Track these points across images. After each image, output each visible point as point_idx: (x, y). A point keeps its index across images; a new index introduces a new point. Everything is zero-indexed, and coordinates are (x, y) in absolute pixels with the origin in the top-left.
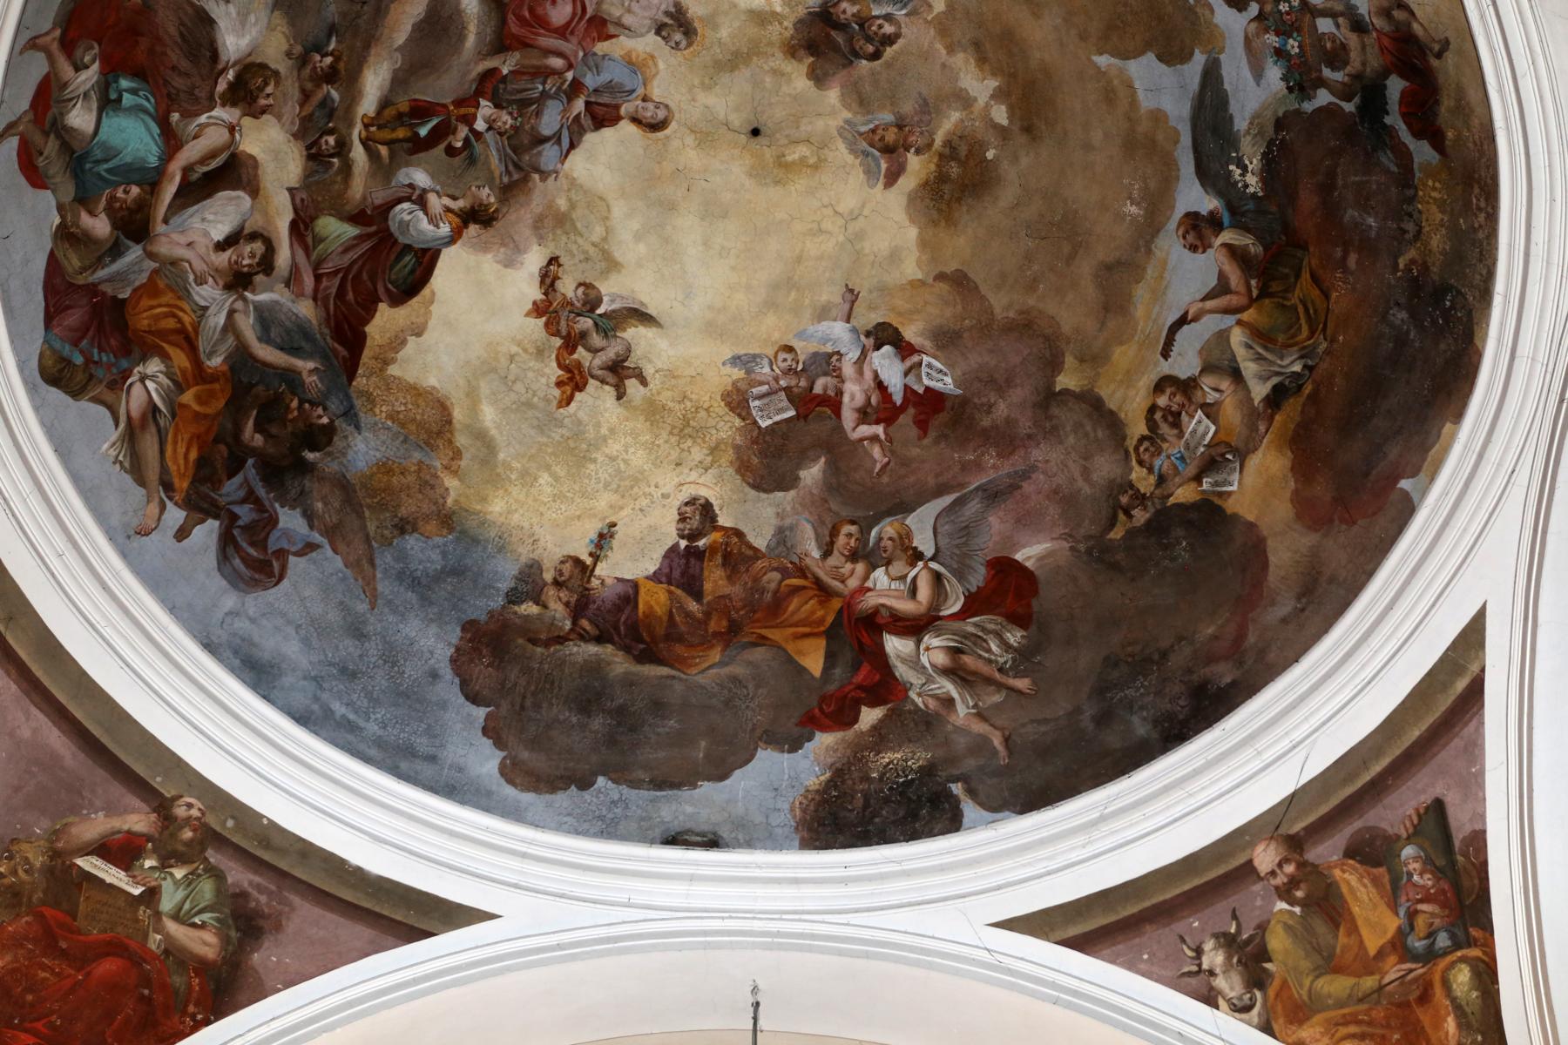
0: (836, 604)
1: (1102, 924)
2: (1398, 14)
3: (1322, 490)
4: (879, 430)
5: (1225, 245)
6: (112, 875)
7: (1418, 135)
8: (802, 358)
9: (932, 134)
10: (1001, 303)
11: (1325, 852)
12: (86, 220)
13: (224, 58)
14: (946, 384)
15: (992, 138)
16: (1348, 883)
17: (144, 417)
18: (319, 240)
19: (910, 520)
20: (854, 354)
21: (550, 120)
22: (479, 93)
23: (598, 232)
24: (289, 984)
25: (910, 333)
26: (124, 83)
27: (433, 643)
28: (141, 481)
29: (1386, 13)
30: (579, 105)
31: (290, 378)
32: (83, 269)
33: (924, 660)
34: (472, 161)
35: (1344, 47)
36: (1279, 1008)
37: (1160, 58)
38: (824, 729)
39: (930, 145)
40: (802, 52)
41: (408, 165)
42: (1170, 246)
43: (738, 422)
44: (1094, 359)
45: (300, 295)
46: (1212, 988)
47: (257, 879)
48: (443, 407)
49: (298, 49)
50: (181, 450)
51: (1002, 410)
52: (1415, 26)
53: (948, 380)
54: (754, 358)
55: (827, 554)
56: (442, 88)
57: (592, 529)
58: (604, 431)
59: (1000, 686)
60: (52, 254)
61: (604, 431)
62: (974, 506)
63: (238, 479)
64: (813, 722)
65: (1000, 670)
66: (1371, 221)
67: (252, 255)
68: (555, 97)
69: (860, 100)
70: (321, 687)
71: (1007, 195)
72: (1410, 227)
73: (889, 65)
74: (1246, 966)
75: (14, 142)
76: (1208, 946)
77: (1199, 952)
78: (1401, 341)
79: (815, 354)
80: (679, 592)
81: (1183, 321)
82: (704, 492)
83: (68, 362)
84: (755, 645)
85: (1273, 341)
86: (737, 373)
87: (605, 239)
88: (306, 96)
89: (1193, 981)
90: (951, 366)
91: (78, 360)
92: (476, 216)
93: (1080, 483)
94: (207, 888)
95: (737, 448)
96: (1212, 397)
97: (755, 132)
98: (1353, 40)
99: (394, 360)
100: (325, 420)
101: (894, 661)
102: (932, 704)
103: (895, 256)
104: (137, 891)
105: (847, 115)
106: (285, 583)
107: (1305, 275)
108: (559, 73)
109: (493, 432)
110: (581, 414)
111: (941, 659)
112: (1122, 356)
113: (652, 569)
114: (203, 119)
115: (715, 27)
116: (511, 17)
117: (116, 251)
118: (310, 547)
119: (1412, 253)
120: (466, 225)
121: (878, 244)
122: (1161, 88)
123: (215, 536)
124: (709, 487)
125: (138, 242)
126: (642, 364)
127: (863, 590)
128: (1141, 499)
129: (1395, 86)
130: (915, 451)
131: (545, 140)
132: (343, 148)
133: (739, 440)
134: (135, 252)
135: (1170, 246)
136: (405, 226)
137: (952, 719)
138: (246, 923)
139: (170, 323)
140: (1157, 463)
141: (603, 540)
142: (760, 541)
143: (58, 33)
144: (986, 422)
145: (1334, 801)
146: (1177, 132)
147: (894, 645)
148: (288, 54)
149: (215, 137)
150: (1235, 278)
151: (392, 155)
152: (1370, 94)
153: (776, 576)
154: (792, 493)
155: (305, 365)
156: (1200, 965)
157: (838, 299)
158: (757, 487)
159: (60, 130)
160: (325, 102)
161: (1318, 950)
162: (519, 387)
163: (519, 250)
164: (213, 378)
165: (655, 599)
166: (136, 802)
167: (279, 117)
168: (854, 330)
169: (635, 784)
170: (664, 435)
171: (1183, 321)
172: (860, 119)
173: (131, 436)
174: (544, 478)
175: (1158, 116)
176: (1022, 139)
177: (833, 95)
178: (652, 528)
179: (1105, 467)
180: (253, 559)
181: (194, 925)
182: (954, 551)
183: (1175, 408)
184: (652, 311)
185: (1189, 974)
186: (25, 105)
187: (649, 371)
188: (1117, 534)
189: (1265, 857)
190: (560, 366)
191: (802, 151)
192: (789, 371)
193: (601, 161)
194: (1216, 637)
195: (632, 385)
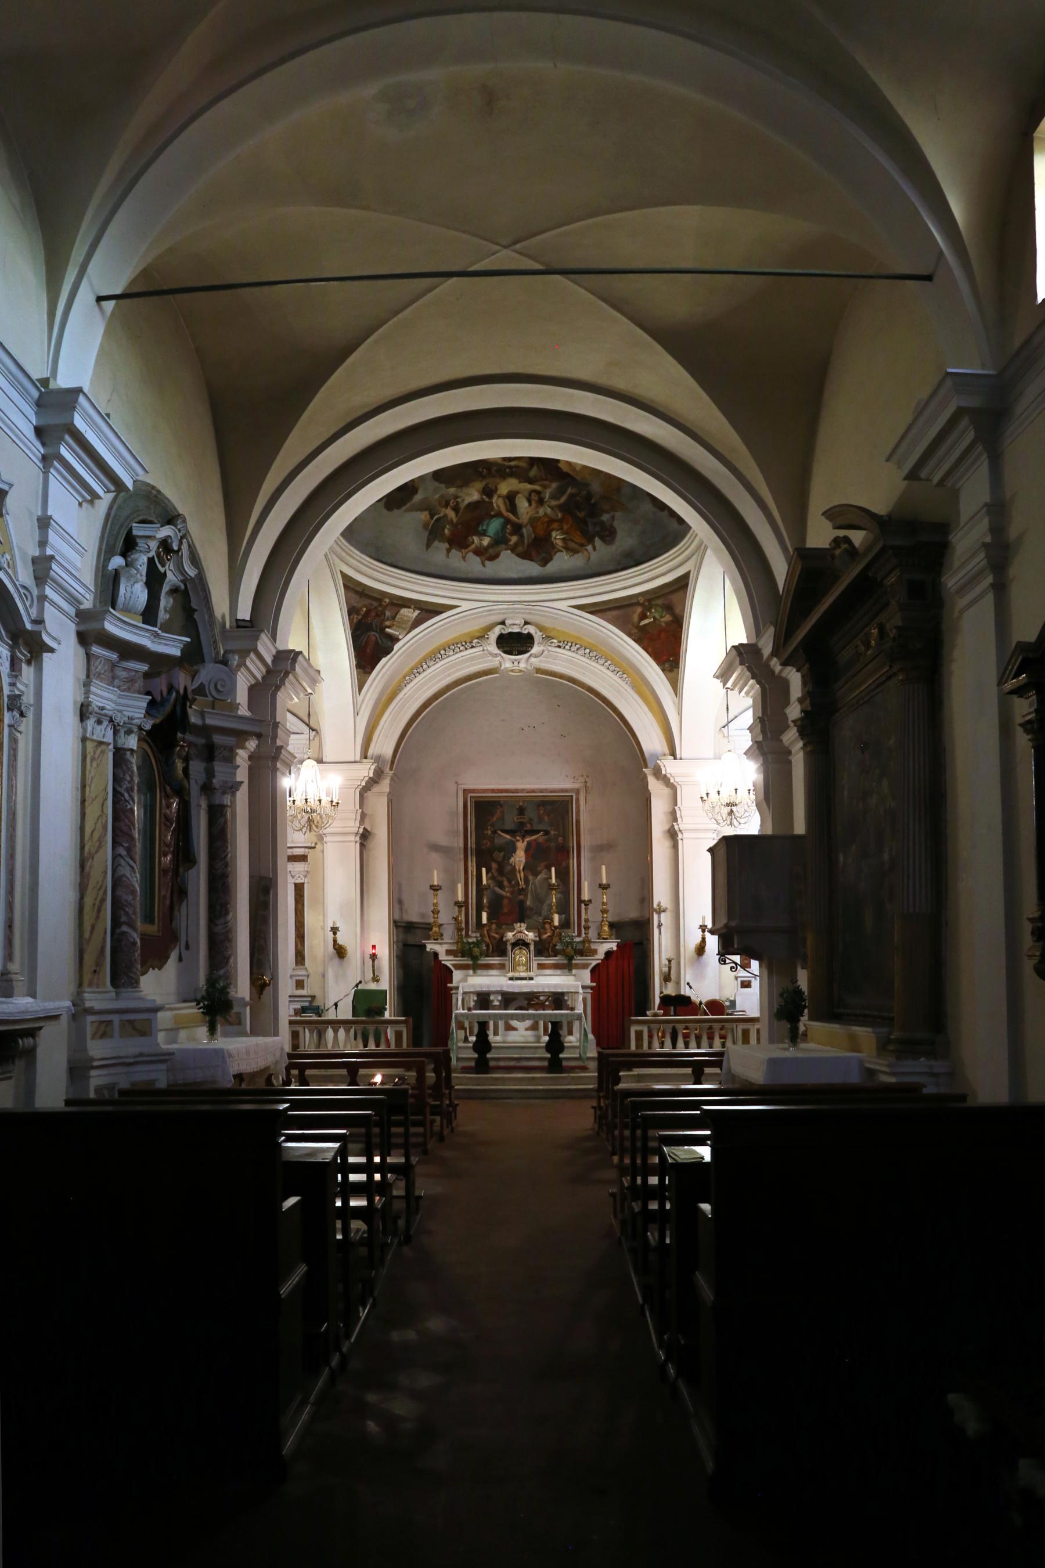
12: (512, 543)
28: (578, 552)
31: (571, 496)
88: (494, 476)
117: (522, 536)
132: (510, 467)
134: (524, 531)
149: (501, 502)
155: (569, 490)
159: (486, 549)
173: (567, 549)
186: (478, 559)
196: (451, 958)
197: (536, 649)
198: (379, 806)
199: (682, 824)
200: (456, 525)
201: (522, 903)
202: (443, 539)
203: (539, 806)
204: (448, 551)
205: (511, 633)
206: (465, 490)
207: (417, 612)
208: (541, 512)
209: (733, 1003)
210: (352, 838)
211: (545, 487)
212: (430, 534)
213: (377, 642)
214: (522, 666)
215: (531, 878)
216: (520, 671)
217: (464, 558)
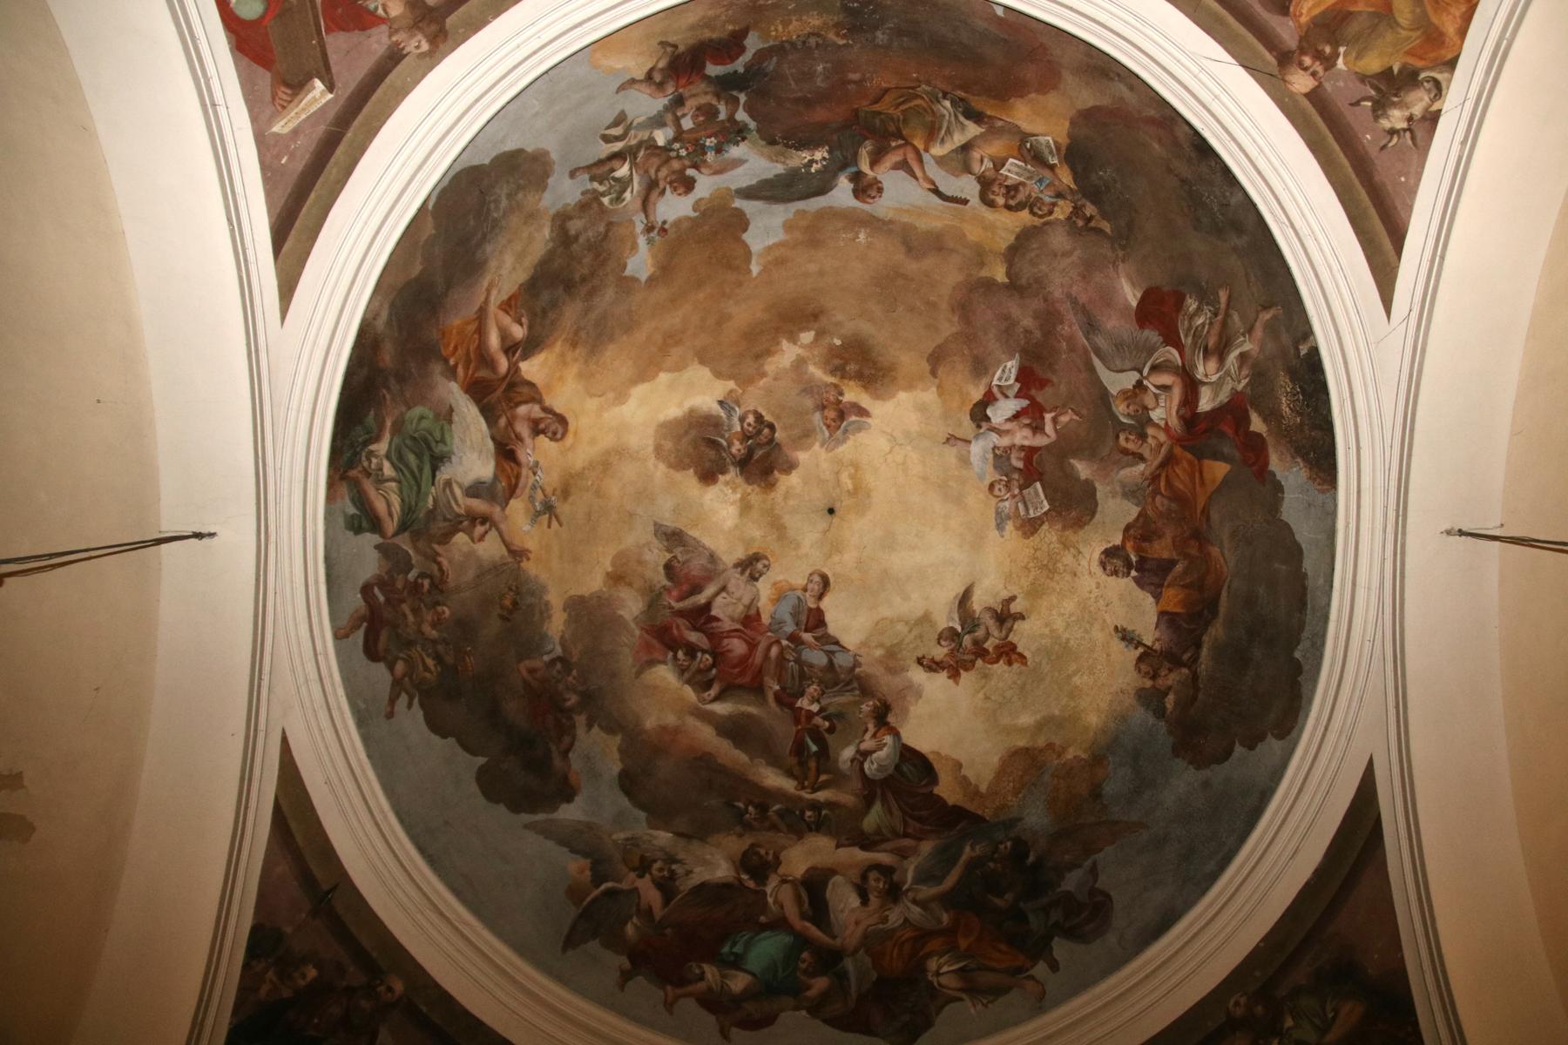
0: (1178, 450)
1: (1379, 221)
2: (657, 77)
3: (1030, 72)
4: (1048, 417)
5: (872, 167)
7: (742, 50)
8: (998, 477)
9: (827, 385)
10: (948, 327)
11: (1287, 31)
12: (812, 993)
13: (731, 880)
14: (1012, 365)
15: (827, 340)
16: (1310, 9)
18: (878, 831)
19: (1114, 391)
20: (994, 437)
21: (817, 658)
22: (791, 706)
24: (1399, 948)
25: (977, 394)
26: (726, 949)
27: (1183, 781)
29: (660, 86)
30: (807, 637)
31: (973, 864)
33: (1214, 378)
34: (840, 716)
35: (698, 109)
36: (1432, 55)
37: (745, 230)
38: (1267, 463)
39: (836, 386)
40: (771, 479)
41: (836, 761)
42: (883, 206)
43: (1045, 527)
44: (980, 255)
45: (915, 851)
46: (1423, 118)
48: (1016, 753)
49: (738, 829)
51: (1027, 322)
52: (661, 65)
53: (1009, 364)
54: (998, 513)
55: (1142, 458)
56: (784, 731)
57: (1118, 646)
58: (1047, 631)
59: (1227, 315)
60: (825, 1021)
61: (1047, 631)
62: (1100, 341)
63: (1031, 918)
64: (1262, 473)
65: (1216, 315)
66: (820, 68)
67: (877, 880)
68: (799, 653)
69: (807, 435)
71: (866, 328)
72: (812, 41)
73: (778, 418)
74: (1399, 89)
75: (734, 1030)
76: (1386, 124)
77: (1392, 132)
78: (899, 32)
79: (995, 467)
80: (1169, 578)
81: (936, 191)
82: (1097, 555)
84: (1208, 519)
85: (933, 123)
86: (1009, 526)
88: (774, 827)
89: (1419, 134)
90: (999, 363)
92: (882, 716)
93: (1074, 257)
95: (1064, 528)
96: (988, 164)
97: (831, 511)
98: (691, 104)
99: (977, 787)
100: (1009, 844)
101: (1216, 403)
102: (1245, 372)
103: (922, 408)
105: (817, 446)
107: (877, 107)
110: (1033, 648)
111: (1212, 365)
112: (973, 234)
113: (1151, 599)
114: (770, 900)
115: (753, 539)
116: (739, 681)
117: (842, 976)
118: (1093, 870)
119: (831, 36)
120: (886, 724)
121: (912, 421)
122: (767, 227)
125: (841, 959)
126: (999, 600)
127: (1167, 429)
128: (1077, 210)
129: (713, 70)
130: (1063, 388)
131: (831, 662)
132: (816, 806)
133: (1059, 526)
134: (849, 964)
135: (883, 206)
136: (881, 768)
137: (1254, 354)
140: (1048, 200)
141: (1126, 637)
142: (1134, 511)
143: (669, 988)
144: (1038, 334)
145: (1242, 30)
146: (798, 212)
147: (1205, 403)
148: (740, 836)
149: (786, 894)
150: (895, 157)
151: (826, 772)
152: (726, 86)
153: (1158, 498)
154: (1097, 485)
156: (1405, 130)
157: (954, 450)
158: (1093, 514)
159: (738, 1000)
160: (780, 814)
161: (1374, 28)
162: (1009, 694)
163: (910, 686)
165: (1173, 598)
167: (784, 848)
168: (977, 437)
169: (1301, 628)
170: (1053, 584)
171: (936, 191)
172: (819, 437)
173: (972, 989)
174: (1076, 680)
175: (788, 226)
176: (824, 321)
177: (802, 456)
178: (1121, 597)
179: (1059, 239)
180: (1088, 916)
181: (1334, 1018)
182: (1133, 354)
183: (1003, 190)
184: (961, 590)
185: (1413, 138)
186: (712, 1019)
187: (1005, 594)
188: (1106, 227)
189: (1301, 83)
190: (997, 661)
192: (1008, 486)
193: (848, 622)
194: (1160, 141)
195: (1015, 608)
202: (615, 941)
204: (626, 977)
206: (695, 845)
208: (895, 917)
211: (903, 854)
212: (581, 916)
217: (669, 1006)
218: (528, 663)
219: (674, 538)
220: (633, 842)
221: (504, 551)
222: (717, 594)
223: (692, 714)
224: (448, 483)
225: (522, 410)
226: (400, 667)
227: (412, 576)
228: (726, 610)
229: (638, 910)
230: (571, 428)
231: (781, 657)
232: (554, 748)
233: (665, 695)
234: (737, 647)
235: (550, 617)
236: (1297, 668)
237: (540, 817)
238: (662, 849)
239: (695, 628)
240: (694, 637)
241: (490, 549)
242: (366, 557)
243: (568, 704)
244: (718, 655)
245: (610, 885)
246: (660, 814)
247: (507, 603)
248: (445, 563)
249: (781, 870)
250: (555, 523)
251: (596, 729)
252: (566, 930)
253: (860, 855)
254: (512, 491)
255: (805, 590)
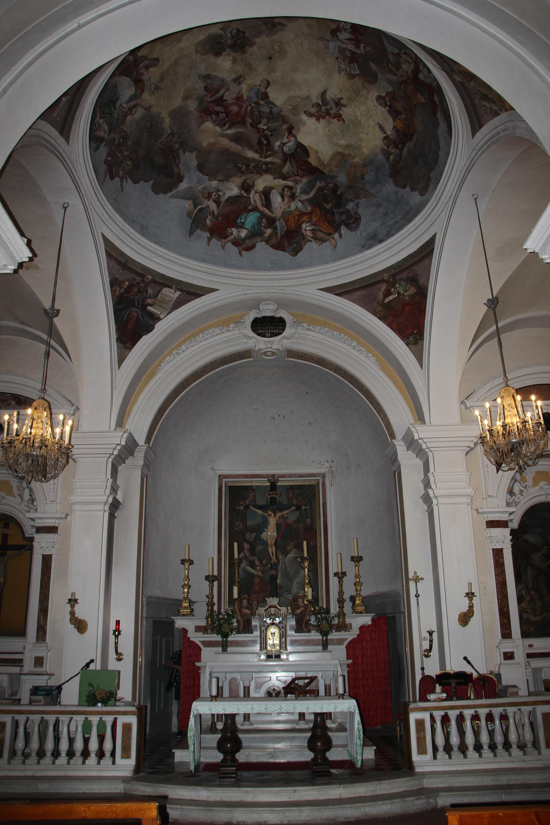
4: (362, 45)
6: (391, 298)
8: (340, 56)
13: (238, 194)
17: (314, 234)
18: (288, 173)
20: (339, 43)
21: (265, 109)
22: (256, 128)
23: (298, 99)
26: (239, 221)
27: (389, 187)
30: (262, 102)
31: (320, 189)
32: (277, 239)
34: (275, 130)
43: (357, 78)
45: (300, 181)
47: (406, 273)
48: (338, 153)
49: (240, 174)
50: (324, 226)
54: (339, 68)
56: (254, 137)
57: (377, 130)
58: (353, 114)
60: (271, 246)
61: (353, 114)
63: (336, 215)
64: (435, 113)
67: (288, 192)
70: (385, 223)
75: (243, 252)
77: (485, 106)
83: (295, 248)
86: (343, 73)
87: (301, 98)
88: (252, 172)
91: (295, 245)
92: (290, 130)
94: (403, 283)
97: (270, 58)
99: (323, 161)
100: (332, 184)
104: (397, 295)
106: (362, 216)
108: (252, 107)
109: (347, 143)
113: (392, 120)
114: (252, 200)
117: (275, 229)
118: (357, 205)
120: (292, 133)
123: (345, 228)
124: (374, 94)
127: (407, 72)
131: (271, 111)
132: (266, 164)
134: (278, 223)
136: (290, 149)
138: (413, 280)
139: (296, 218)
142: (390, 89)
143: (223, 240)
148: (240, 177)
151: (270, 151)
155: (318, 185)
160: (254, 167)
162: (337, 131)
163: (301, 121)
164: (312, 211)
166: (380, 285)
167: (256, 180)
168: (332, 41)
173: (315, 238)
177: (258, 40)
180: (353, 221)
184: (323, 90)
186: (235, 249)
187: (339, 96)
190: (334, 118)
191: (276, 47)
192: (344, 60)
193: (278, 97)
195: (342, 102)
196: (200, 634)
197: (288, 331)
198: (132, 474)
199: (436, 490)
200: (216, 217)
201: (274, 578)
202: (204, 228)
203: (288, 489)
204: (209, 240)
205: (264, 318)
206: (226, 183)
207: (178, 293)
208: (293, 206)
209: (499, 676)
210: (101, 507)
211: (296, 182)
212: (193, 222)
213: (138, 317)
214: (275, 346)
215: (280, 557)
216: (273, 354)
217: (223, 247)
218: (159, 141)
219: (207, 77)
220: (205, 188)
221: (144, 110)
222: (225, 92)
223: (220, 136)
224: (121, 105)
225: (141, 65)
226: (121, 173)
227: (116, 143)
228: (229, 97)
229: (210, 213)
230: (161, 59)
231: (252, 111)
232: (173, 165)
233: (210, 134)
234: (235, 109)
235: (164, 122)
236: (429, 179)
237: (174, 191)
238: (214, 188)
239: (218, 106)
240: (217, 109)
241: (139, 113)
242: (103, 151)
243: (176, 148)
244: (227, 113)
245: (199, 207)
246: (212, 175)
247: (149, 126)
248: (125, 129)
249: (255, 188)
250: (160, 91)
251: (187, 153)
252: (189, 230)
253: (282, 182)
254: (142, 91)
255: (260, 86)
